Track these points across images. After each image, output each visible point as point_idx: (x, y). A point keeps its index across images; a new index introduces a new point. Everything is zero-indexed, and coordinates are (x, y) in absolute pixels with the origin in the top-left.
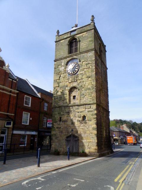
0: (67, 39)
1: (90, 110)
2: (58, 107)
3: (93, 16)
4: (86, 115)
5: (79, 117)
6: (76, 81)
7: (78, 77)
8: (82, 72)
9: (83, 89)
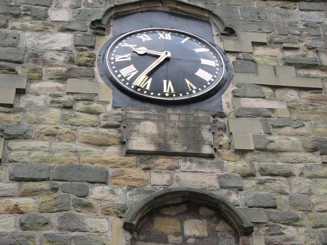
6: (207, 150)
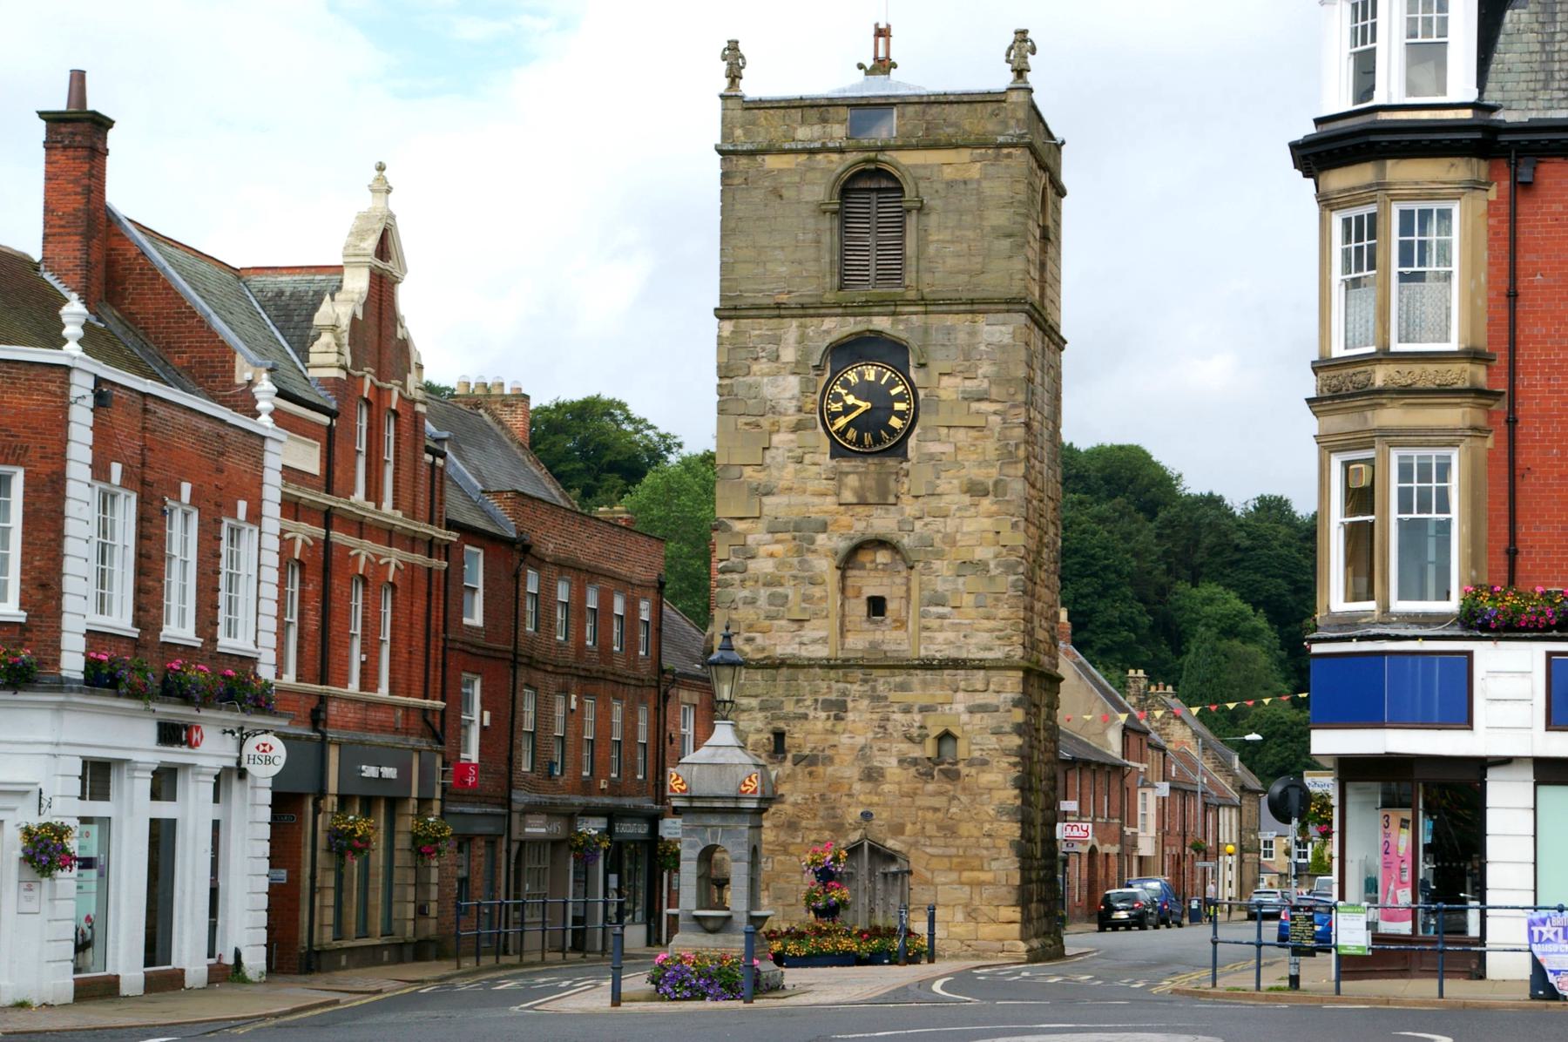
0: (820, 157)
1: (980, 699)
2: (761, 666)
3: (1022, 35)
4: (956, 731)
5: (910, 739)
7: (907, 475)
8: (934, 448)
9: (937, 564)
